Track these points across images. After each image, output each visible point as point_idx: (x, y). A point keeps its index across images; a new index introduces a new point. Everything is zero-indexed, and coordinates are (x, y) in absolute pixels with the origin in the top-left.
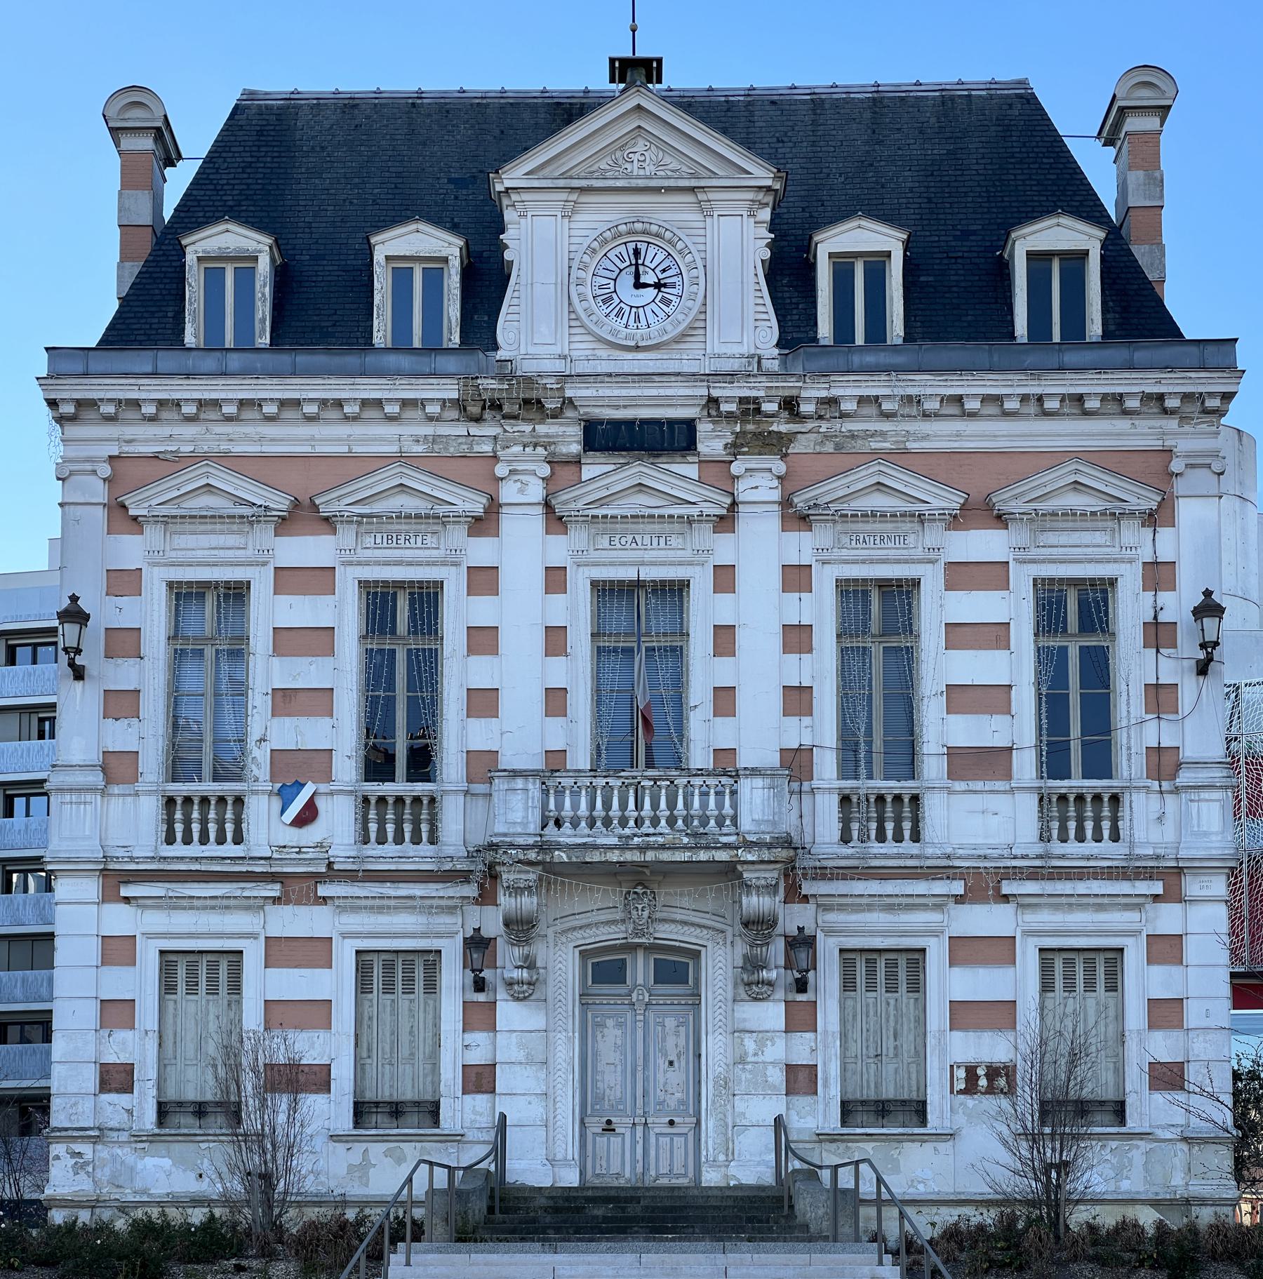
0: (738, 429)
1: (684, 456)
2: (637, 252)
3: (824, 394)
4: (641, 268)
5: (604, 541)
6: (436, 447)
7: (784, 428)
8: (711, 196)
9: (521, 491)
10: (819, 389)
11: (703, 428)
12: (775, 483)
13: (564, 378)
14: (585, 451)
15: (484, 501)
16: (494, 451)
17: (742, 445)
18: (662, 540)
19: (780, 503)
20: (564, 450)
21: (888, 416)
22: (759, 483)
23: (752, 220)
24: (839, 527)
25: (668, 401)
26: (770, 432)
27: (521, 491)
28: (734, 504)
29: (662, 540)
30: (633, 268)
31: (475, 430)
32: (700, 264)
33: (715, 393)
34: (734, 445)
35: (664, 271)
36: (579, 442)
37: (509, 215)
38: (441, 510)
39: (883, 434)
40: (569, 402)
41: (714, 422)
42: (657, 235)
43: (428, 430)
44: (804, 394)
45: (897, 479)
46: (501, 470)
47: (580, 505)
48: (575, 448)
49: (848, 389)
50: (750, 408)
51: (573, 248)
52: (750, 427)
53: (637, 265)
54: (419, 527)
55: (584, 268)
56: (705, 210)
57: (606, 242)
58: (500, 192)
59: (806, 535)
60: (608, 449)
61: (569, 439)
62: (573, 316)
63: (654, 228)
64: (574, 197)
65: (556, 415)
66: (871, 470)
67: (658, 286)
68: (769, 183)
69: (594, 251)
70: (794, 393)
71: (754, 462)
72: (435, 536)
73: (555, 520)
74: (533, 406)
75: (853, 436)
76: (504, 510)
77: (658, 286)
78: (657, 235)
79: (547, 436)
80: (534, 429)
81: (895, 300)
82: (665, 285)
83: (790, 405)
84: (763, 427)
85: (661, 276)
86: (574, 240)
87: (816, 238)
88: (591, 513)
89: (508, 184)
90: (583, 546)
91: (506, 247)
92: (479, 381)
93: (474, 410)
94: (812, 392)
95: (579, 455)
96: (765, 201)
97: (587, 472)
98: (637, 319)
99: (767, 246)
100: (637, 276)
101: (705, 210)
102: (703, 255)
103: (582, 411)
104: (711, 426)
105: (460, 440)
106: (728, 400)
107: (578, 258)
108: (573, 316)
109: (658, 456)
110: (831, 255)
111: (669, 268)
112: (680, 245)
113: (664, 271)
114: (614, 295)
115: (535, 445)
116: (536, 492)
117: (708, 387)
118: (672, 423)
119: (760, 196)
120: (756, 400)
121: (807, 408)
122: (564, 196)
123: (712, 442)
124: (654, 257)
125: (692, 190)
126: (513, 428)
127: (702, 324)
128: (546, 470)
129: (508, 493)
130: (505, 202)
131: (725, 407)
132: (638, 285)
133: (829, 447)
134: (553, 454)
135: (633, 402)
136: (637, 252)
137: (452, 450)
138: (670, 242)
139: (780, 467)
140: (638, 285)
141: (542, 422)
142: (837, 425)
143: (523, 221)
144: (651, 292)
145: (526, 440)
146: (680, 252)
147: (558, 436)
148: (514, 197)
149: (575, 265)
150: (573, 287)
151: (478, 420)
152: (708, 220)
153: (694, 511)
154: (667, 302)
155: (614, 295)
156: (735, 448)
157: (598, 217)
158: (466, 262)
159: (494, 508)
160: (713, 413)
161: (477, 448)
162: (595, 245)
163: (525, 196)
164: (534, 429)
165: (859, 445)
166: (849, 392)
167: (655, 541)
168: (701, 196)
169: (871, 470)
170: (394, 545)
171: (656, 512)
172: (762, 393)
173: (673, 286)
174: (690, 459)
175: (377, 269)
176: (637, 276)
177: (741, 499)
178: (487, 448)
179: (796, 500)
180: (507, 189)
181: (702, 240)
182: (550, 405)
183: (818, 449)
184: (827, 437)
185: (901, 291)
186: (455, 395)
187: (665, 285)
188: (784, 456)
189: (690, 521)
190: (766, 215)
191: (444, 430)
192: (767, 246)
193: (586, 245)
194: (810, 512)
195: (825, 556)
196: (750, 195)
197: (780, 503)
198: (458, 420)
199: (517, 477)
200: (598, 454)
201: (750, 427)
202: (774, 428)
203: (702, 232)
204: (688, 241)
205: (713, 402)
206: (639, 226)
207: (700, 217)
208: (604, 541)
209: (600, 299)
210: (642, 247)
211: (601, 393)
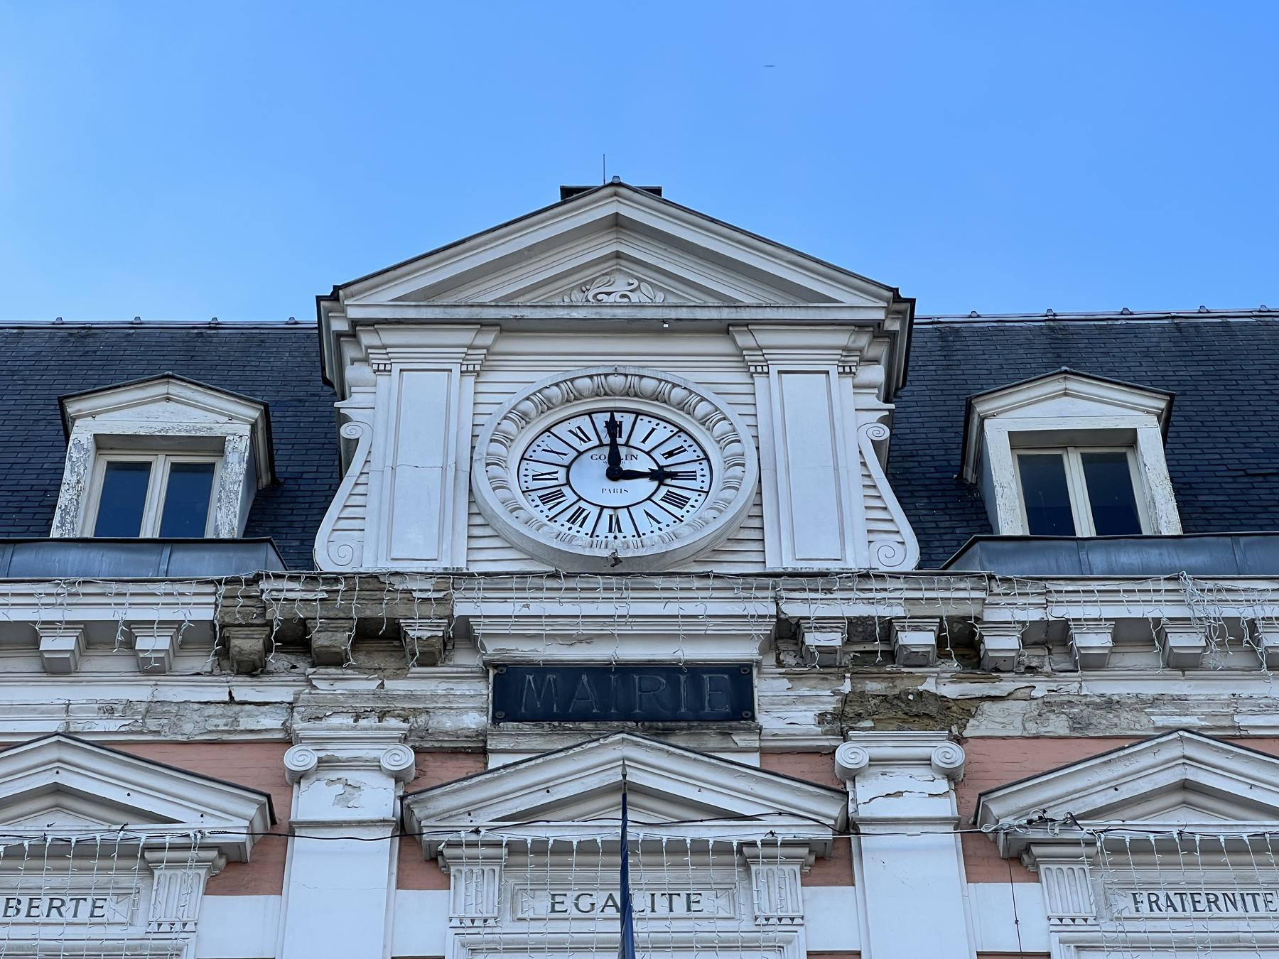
0: (847, 687)
1: (726, 734)
2: (613, 427)
3: (1035, 615)
4: (623, 451)
5: (541, 905)
6: (152, 724)
7: (951, 691)
8: (765, 338)
9: (342, 800)
10: (1024, 607)
11: (766, 688)
12: (943, 785)
13: (454, 577)
14: (495, 720)
15: (252, 811)
16: (286, 729)
17: (859, 717)
18: (680, 903)
19: (957, 823)
20: (448, 723)
21: (1183, 664)
22: (903, 784)
23: (848, 381)
24: (1108, 876)
25: (690, 628)
26: (920, 695)
27: (342, 800)
28: (849, 827)
29: (680, 903)
30: (606, 451)
31: (246, 690)
32: (745, 434)
33: (792, 610)
34: (839, 716)
35: (670, 454)
36: (482, 710)
37: (353, 373)
38: (143, 833)
39: (1180, 700)
40: (463, 633)
41: (793, 677)
42: (656, 397)
43: (140, 693)
44: (989, 615)
45: (1230, 773)
46: (296, 758)
47: (482, 820)
48: (474, 720)
49: (1090, 611)
50: (872, 643)
51: (479, 420)
52: (873, 686)
53: (614, 446)
54: (84, 880)
55: (507, 440)
56: (751, 365)
57: (549, 405)
58: (339, 335)
59: (1026, 890)
60: (549, 717)
61: (462, 703)
62: (475, 510)
63: (649, 385)
64: (487, 339)
65: (432, 656)
66: (1165, 755)
67: (659, 475)
68: (880, 315)
69: (524, 416)
70: (972, 610)
71: (889, 744)
72: (126, 902)
73: (420, 854)
74: (380, 638)
75: (1110, 704)
76: (298, 845)
77: (659, 475)
78: (656, 397)
79: (410, 696)
80: (382, 685)
81: (1159, 500)
82: (673, 476)
83: (962, 643)
84: (902, 685)
85: (663, 462)
86: (480, 409)
87: (982, 408)
88: (505, 836)
89: (354, 313)
90: (489, 909)
91: (345, 419)
92: (263, 585)
93: (247, 644)
94: (1007, 616)
95: (482, 735)
96: (871, 353)
97: (494, 761)
98: (615, 525)
99: (882, 420)
100: (614, 459)
101: (751, 365)
102: (751, 421)
103: (491, 647)
104: (786, 683)
105: (211, 710)
106: (823, 623)
107: (489, 424)
108: (478, 520)
109: (667, 732)
110: (1016, 439)
111: (681, 450)
112: (702, 409)
113: (670, 454)
114: (566, 490)
115: (382, 715)
116: (379, 799)
117: (776, 600)
118: (696, 671)
119: (863, 340)
120: (888, 628)
121: (998, 644)
122: (466, 337)
123: (788, 708)
124: (646, 442)
125: (725, 329)
126: (329, 685)
127: (755, 535)
128: (404, 758)
129: (310, 802)
130: (349, 352)
131: (813, 639)
132: (616, 473)
133: (1059, 725)
134: (426, 732)
135: (605, 629)
136: (613, 427)
137: (188, 728)
138: (681, 406)
139: (949, 753)
140: (616, 473)
141: (401, 673)
142: (1071, 685)
143: (382, 380)
144: (647, 486)
145: (360, 705)
146: (703, 421)
147: (434, 697)
148: (367, 339)
149: (485, 434)
150: (479, 468)
151: (253, 669)
152: (758, 380)
153: (755, 834)
154: (681, 502)
155: (566, 490)
156: (841, 721)
157: (528, 372)
158: (265, 480)
159: (276, 832)
160: (789, 659)
161: (245, 723)
162: (527, 406)
163: (389, 337)
164: (382, 685)
165: (1126, 722)
166: (1092, 612)
167: (662, 903)
168: (743, 340)
169: (1165, 755)
170: (22, 918)
171: (664, 835)
172: (899, 611)
173: (692, 476)
174: (741, 740)
175: (73, 453)
176: (614, 459)
177: (864, 812)
178: (270, 722)
179: (996, 809)
180: (355, 323)
181: (750, 410)
182: (416, 632)
183: (1033, 728)
184: (1049, 705)
185: (1173, 503)
186: (207, 614)
187: (673, 476)
188: (959, 740)
189: (743, 857)
190: (877, 374)
191: (173, 692)
192: (882, 420)
193: (507, 407)
194: (1035, 834)
195: (1083, 933)
196: (842, 339)
197: (957, 823)
198: (211, 674)
199: (334, 775)
200: (526, 727)
201: (873, 686)
202: (929, 686)
203: (749, 399)
204: (720, 402)
205: (787, 633)
206: (617, 382)
207: (744, 378)
208: (541, 905)
209: (535, 495)
210: (626, 420)
211: (535, 609)
